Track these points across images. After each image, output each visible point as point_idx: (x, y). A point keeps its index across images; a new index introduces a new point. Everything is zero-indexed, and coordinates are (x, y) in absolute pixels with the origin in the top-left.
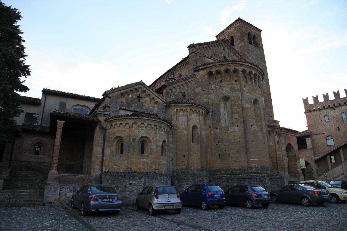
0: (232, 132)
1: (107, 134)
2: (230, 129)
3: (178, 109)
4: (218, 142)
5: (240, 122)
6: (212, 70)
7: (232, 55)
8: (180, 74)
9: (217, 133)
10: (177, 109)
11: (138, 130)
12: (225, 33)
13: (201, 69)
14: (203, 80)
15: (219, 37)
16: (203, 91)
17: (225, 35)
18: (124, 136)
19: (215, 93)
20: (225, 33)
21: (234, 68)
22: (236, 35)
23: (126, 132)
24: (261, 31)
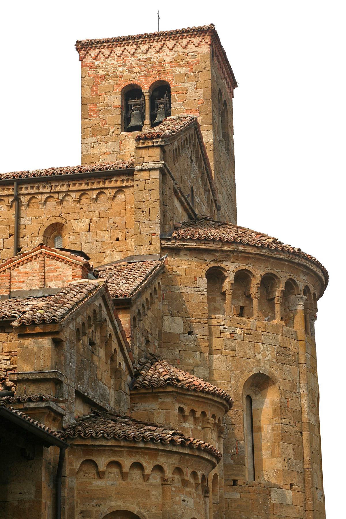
0: (277, 505)
1: (65, 493)
2: (273, 495)
3: (185, 408)
5: (298, 472)
6: (224, 265)
8: (59, 220)
9: (235, 500)
10: (181, 410)
11: (182, 497)
13: (191, 250)
14: (192, 291)
16: (190, 333)
17: (131, 61)
19: (232, 353)
21: (289, 277)
23: (153, 499)
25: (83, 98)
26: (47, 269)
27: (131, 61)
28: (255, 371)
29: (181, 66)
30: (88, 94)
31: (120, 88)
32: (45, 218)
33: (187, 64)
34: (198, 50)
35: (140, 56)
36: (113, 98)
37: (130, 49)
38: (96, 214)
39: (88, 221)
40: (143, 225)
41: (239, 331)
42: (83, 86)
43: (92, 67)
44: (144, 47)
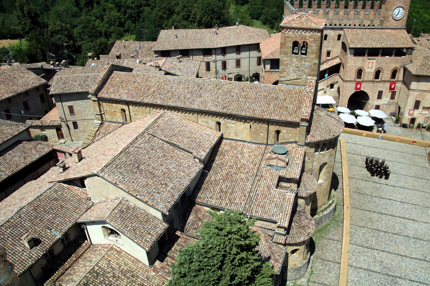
8: (279, 129)
15: (285, 30)
17: (297, 34)
22: (312, 44)
25: (281, 42)
27: (297, 34)
30: (283, 41)
34: (317, 34)
35: (299, 33)
37: (297, 31)
41: (321, 156)
42: (281, 39)
44: (301, 31)
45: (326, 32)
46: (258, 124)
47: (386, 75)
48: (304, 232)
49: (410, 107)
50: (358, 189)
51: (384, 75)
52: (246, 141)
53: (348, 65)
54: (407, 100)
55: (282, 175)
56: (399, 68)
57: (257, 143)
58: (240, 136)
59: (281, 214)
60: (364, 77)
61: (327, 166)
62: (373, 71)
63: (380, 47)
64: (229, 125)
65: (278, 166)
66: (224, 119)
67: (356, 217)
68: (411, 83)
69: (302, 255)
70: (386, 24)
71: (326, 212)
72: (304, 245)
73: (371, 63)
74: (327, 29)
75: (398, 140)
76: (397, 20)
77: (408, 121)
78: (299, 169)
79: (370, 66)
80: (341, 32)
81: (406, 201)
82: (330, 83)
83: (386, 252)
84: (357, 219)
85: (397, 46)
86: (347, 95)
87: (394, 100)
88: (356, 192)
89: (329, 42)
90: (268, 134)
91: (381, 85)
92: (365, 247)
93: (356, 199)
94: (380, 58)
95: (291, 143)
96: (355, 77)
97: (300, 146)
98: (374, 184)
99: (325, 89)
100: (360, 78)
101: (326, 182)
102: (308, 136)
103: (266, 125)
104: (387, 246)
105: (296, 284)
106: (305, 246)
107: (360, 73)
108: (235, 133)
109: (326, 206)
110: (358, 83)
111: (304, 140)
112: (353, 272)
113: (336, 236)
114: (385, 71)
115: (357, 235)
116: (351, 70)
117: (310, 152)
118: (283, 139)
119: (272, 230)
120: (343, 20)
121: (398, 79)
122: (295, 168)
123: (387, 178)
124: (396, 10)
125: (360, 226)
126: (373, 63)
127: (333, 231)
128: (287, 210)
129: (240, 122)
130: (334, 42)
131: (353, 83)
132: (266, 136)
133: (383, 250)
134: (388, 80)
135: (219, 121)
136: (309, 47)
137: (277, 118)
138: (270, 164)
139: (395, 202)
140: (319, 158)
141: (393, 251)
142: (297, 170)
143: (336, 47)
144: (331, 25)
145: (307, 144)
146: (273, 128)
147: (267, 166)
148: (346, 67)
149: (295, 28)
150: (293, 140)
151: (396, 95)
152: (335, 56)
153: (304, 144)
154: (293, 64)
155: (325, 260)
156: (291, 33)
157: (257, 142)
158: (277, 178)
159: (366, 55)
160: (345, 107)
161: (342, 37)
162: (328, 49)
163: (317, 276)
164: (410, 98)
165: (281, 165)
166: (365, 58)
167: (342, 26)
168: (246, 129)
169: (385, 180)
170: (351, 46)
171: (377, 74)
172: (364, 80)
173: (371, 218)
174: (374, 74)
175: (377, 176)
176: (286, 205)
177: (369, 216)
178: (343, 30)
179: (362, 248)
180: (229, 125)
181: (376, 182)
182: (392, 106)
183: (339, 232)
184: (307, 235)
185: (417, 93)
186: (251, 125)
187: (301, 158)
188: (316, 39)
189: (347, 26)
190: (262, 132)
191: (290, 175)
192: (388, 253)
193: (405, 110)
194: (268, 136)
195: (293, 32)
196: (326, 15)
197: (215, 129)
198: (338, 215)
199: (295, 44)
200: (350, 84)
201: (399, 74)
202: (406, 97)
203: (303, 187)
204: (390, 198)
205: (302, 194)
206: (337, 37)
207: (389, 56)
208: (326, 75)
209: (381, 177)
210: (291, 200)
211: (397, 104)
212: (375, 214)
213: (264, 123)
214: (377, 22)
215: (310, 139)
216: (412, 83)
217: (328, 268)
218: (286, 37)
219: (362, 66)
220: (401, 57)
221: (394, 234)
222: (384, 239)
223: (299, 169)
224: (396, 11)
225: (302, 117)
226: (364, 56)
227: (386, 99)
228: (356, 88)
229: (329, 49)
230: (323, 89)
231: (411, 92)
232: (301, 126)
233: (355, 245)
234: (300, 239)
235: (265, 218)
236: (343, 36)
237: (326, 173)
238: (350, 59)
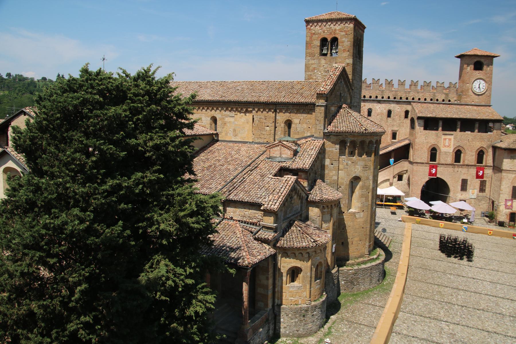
3: (325, 206)
4: (343, 229)
7: (345, 86)
8: (290, 119)
10: (323, 207)
12: (325, 26)
15: (311, 24)
16: (332, 164)
17: (324, 28)
18: (303, 266)
19: (346, 170)
20: (325, 26)
22: (344, 39)
24: (364, 28)
25: (306, 41)
26: (282, 150)
28: (354, 175)
29: (342, 32)
30: (308, 40)
31: (320, 38)
32: (285, 117)
33: (345, 31)
34: (349, 26)
35: (327, 26)
36: (317, 42)
37: (324, 24)
38: (302, 117)
39: (299, 120)
40: (318, 126)
41: (350, 162)
43: (310, 29)
44: (329, 23)
45: (390, 106)
46: (262, 112)
47: (469, 157)
48: (310, 238)
49: (506, 195)
50: (424, 265)
51: (467, 157)
52: (247, 142)
53: (417, 140)
54: (500, 186)
55: (285, 165)
56: (486, 148)
57: (261, 143)
58: (239, 135)
59: (271, 196)
60: (440, 158)
61: (361, 183)
62: (452, 151)
63: (457, 117)
64: (227, 119)
65: (282, 158)
66: (220, 111)
67: (416, 289)
68: (502, 162)
69: (308, 286)
70: (465, 100)
71: (363, 266)
72: (310, 263)
73: (447, 140)
74: (391, 103)
75: (490, 233)
76: (479, 95)
77: (505, 216)
78: (312, 159)
79: (447, 144)
80: (409, 108)
81: (500, 282)
82: (396, 172)
83: (462, 325)
84: (417, 290)
85: (479, 118)
86: (419, 183)
87: (484, 194)
88: (421, 268)
89: (393, 119)
90: (276, 127)
91: (464, 170)
92: (425, 317)
93: (420, 274)
94: (458, 133)
95: (306, 138)
96: (428, 158)
97: (317, 139)
98: (450, 265)
99: (390, 179)
100: (435, 161)
101: (362, 214)
102: (329, 126)
103: (273, 113)
104: (463, 320)
105: (297, 342)
106: (312, 264)
107: (433, 153)
108: (234, 130)
109: (366, 259)
110: (432, 167)
111: (322, 128)
112: (400, 339)
113: (379, 302)
114: (467, 151)
115: (416, 304)
116: (422, 148)
117: (332, 151)
118: (296, 134)
119: (256, 225)
120: (410, 92)
121: (486, 163)
122: (306, 158)
123: (470, 259)
124: (476, 82)
125: (422, 297)
126: (450, 139)
127: (376, 297)
128: (281, 191)
129: (240, 112)
130: (400, 120)
131: (426, 166)
132: (273, 131)
133: (457, 323)
134: (473, 164)
135: (215, 115)
136: (340, 44)
137: (287, 100)
138: (272, 155)
139: (481, 281)
140: (347, 165)
141: (474, 326)
142: (308, 160)
143: (403, 126)
144: (395, 98)
145: (327, 136)
146: (282, 117)
147: (267, 158)
148: (415, 144)
149: (321, 21)
150: (309, 134)
151: (487, 186)
152: (402, 138)
153: (322, 134)
154: (322, 68)
155: (356, 323)
156: (318, 27)
157: (262, 142)
158: (277, 168)
159: (440, 128)
160: (417, 197)
161: (410, 113)
162: (393, 129)
163: (336, 338)
164: (504, 183)
165: (286, 156)
166: (439, 133)
167: (410, 99)
168: (248, 124)
169: (468, 262)
170: (420, 115)
171: (458, 155)
172: (441, 163)
173: (440, 292)
174: (453, 155)
175: (455, 257)
176: (281, 186)
177: (437, 290)
178: (410, 104)
179: (421, 317)
180: (227, 119)
181: (453, 263)
182: (483, 202)
183: (385, 299)
184: (313, 241)
185: (513, 176)
186: (253, 116)
187: (317, 149)
188: (348, 33)
189: (416, 100)
190: (267, 124)
191: (297, 165)
192: (466, 327)
193: (500, 201)
194: (275, 130)
195: (320, 26)
196: (388, 85)
197: (209, 128)
198: (387, 284)
199: (324, 41)
200: (422, 167)
201: (487, 157)
202: (498, 183)
203: (318, 189)
204: (474, 277)
205: (314, 198)
206: (403, 114)
207: (471, 132)
208: (392, 160)
209: (461, 259)
210: (290, 182)
211: (490, 199)
212: (448, 288)
213: (270, 110)
214: (453, 96)
215: (330, 128)
216: (505, 160)
217: (358, 331)
218: (311, 33)
219: (436, 143)
220: (487, 134)
221: (478, 309)
222: (460, 313)
223: (312, 159)
224: (476, 84)
225: (319, 92)
226: (437, 130)
227: (473, 192)
228: (430, 174)
229: (395, 128)
230: (388, 180)
231: (504, 174)
232: (318, 106)
233: (410, 314)
234: (301, 244)
235: (246, 200)
236: (411, 111)
237: (362, 196)
238: (420, 133)
